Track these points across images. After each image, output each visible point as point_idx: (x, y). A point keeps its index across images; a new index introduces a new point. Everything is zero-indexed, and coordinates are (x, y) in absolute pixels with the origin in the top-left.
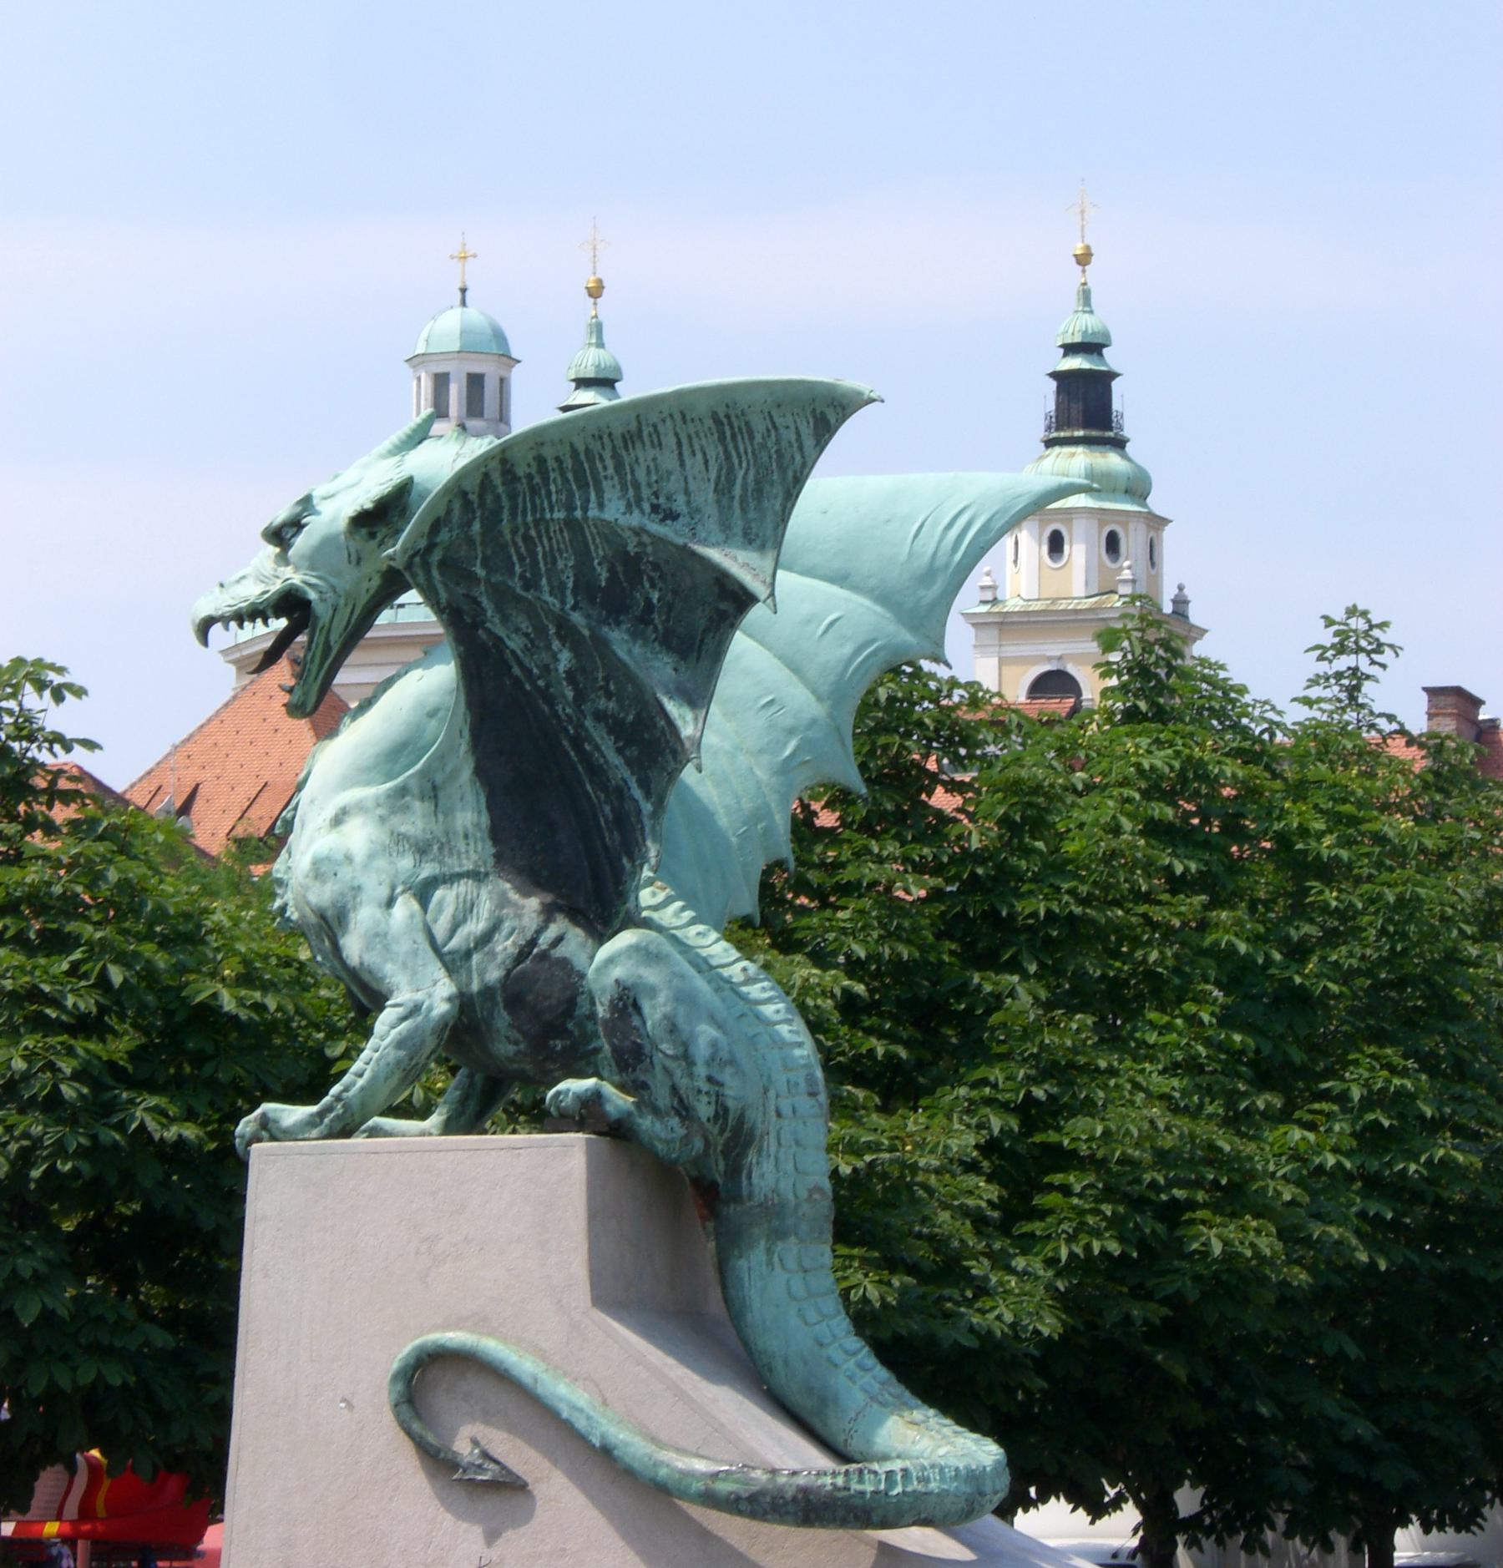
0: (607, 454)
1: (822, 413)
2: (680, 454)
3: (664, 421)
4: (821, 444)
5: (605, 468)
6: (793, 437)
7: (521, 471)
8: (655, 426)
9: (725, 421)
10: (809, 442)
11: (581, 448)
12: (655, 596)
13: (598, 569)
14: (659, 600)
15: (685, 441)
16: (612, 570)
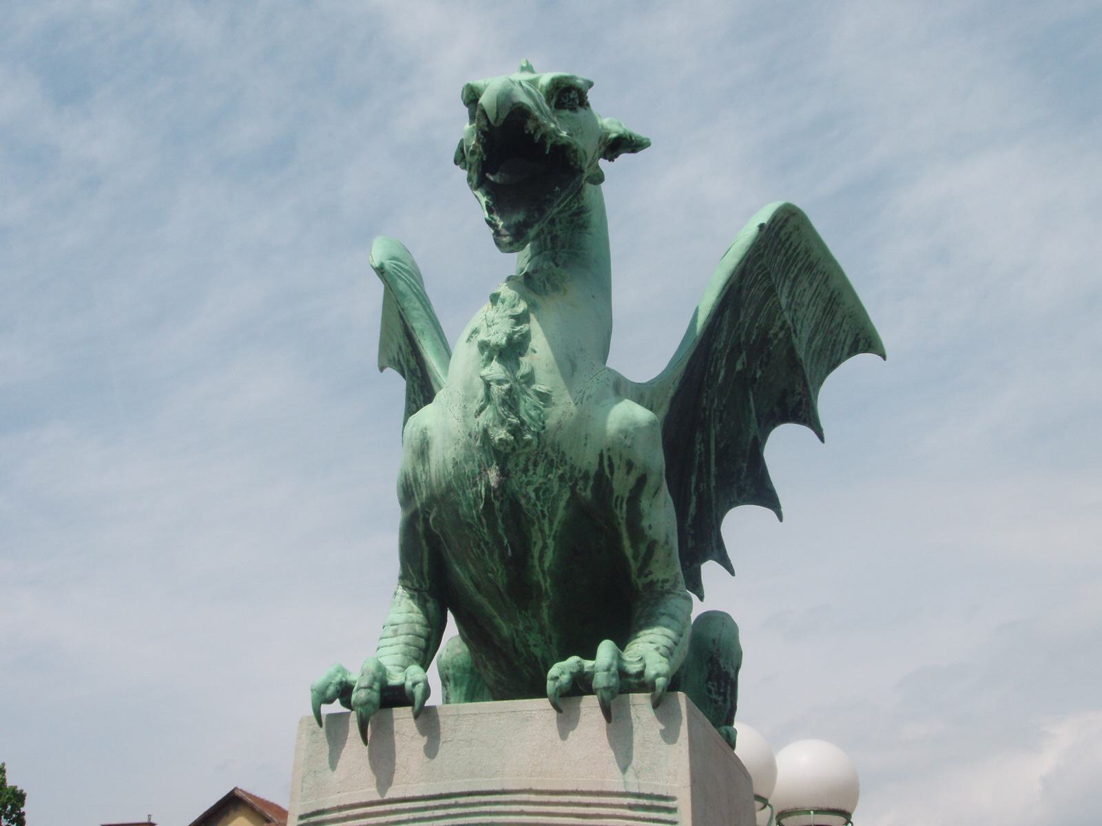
0: (799, 265)
1: (860, 339)
2: (810, 301)
3: (821, 273)
4: (850, 355)
5: (792, 273)
6: (843, 340)
7: (782, 233)
8: (817, 272)
9: (832, 300)
10: (846, 350)
11: (798, 251)
12: (759, 374)
13: (755, 330)
14: (760, 377)
15: (816, 294)
16: (757, 336)
